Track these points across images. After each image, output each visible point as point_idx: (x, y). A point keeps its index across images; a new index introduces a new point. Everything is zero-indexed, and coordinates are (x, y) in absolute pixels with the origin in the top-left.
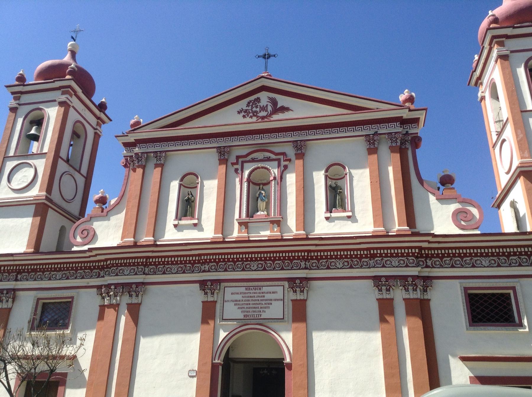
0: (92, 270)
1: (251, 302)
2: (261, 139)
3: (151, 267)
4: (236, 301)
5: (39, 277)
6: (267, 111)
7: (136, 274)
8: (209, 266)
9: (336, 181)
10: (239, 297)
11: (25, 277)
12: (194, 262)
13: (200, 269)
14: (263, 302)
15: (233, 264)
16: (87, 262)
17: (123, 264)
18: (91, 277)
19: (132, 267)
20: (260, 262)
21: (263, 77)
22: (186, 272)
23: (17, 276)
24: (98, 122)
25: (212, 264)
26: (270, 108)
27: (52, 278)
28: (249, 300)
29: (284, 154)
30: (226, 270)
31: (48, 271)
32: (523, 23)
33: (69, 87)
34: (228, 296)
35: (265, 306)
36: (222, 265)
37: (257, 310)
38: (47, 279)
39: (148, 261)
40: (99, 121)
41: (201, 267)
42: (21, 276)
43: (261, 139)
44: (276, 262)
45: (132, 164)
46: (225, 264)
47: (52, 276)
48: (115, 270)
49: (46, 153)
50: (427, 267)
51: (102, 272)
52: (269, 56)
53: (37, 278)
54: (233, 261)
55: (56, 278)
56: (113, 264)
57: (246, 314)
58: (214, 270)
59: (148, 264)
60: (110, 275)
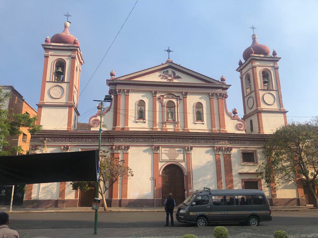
0: (105, 139)
6: (171, 77)
7: (126, 141)
9: (199, 109)
10: (167, 152)
12: (149, 138)
23: (69, 140)
26: (172, 76)
28: (171, 153)
29: (179, 96)
31: (84, 138)
32: (260, 54)
34: (163, 152)
49: (69, 82)
50: (231, 143)
54: (164, 138)
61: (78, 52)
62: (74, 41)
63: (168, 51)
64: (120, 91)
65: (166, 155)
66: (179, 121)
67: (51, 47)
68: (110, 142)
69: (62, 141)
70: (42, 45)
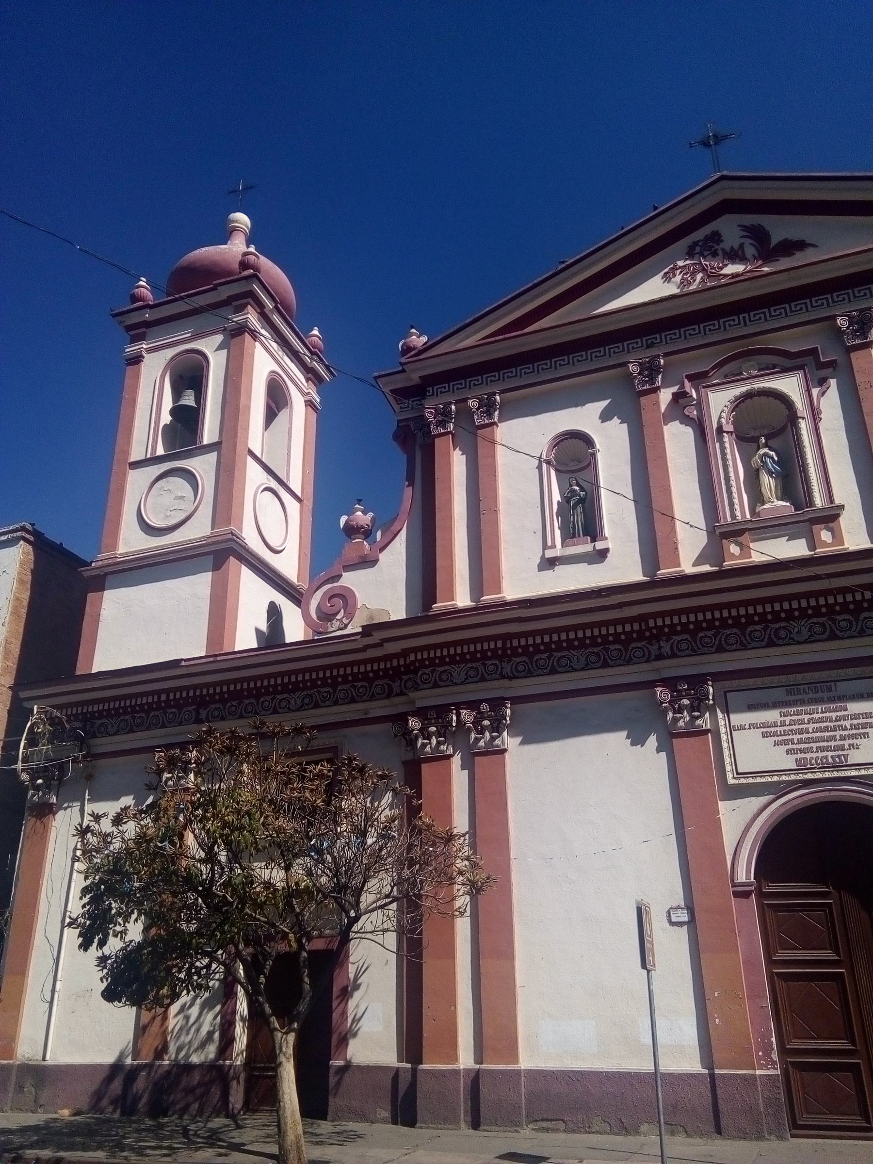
0: (370, 681)
1: (811, 726)
2: (745, 325)
3: (518, 660)
4: (764, 725)
5: (250, 709)
7: (483, 679)
8: (670, 643)
11: (216, 713)
13: (647, 654)
14: (847, 723)
15: (739, 633)
16: (358, 663)
17: (447, 660)
18: (372, 698)
19: (469, 665)
20: (815, 620)
21: (723, 178)
22: (611, 663)
23: (198, 713)
24: (307, 380)
25: (679, 638)
26: (750, 251)
27: (280, 708)
29: (813, 352)
30: (720, 649)
31: (268, 693)
33: (252, 294)
35: (854, 732)
36: (706, 636)
37: (833, 744)
38: (268, 712)
39: (509, 645)
40: (310, 375)
41: (650, 647)
42: (206, 711)
43: (745, 325)
44: (865, 614)
45: (419, 435)
46: (715, 635)
47: (279, 704)
48: (428, 674)
51: (397, 683)
52: (719, 139)
53: (246, 712)
55: (289, 708)
56: (423, 660)
57: (799, 756)
58: (687, 652)
59: (509, 652)
60: (420, 687)
61: (260, 305)
62: (240, 258)
63: (706, 144)
64: (444, 416)
65: (764, 735)
66: (837, 501)
67: (147, 316)
68: (397, 695)
69: (163, 726)
70: (115, 316)
